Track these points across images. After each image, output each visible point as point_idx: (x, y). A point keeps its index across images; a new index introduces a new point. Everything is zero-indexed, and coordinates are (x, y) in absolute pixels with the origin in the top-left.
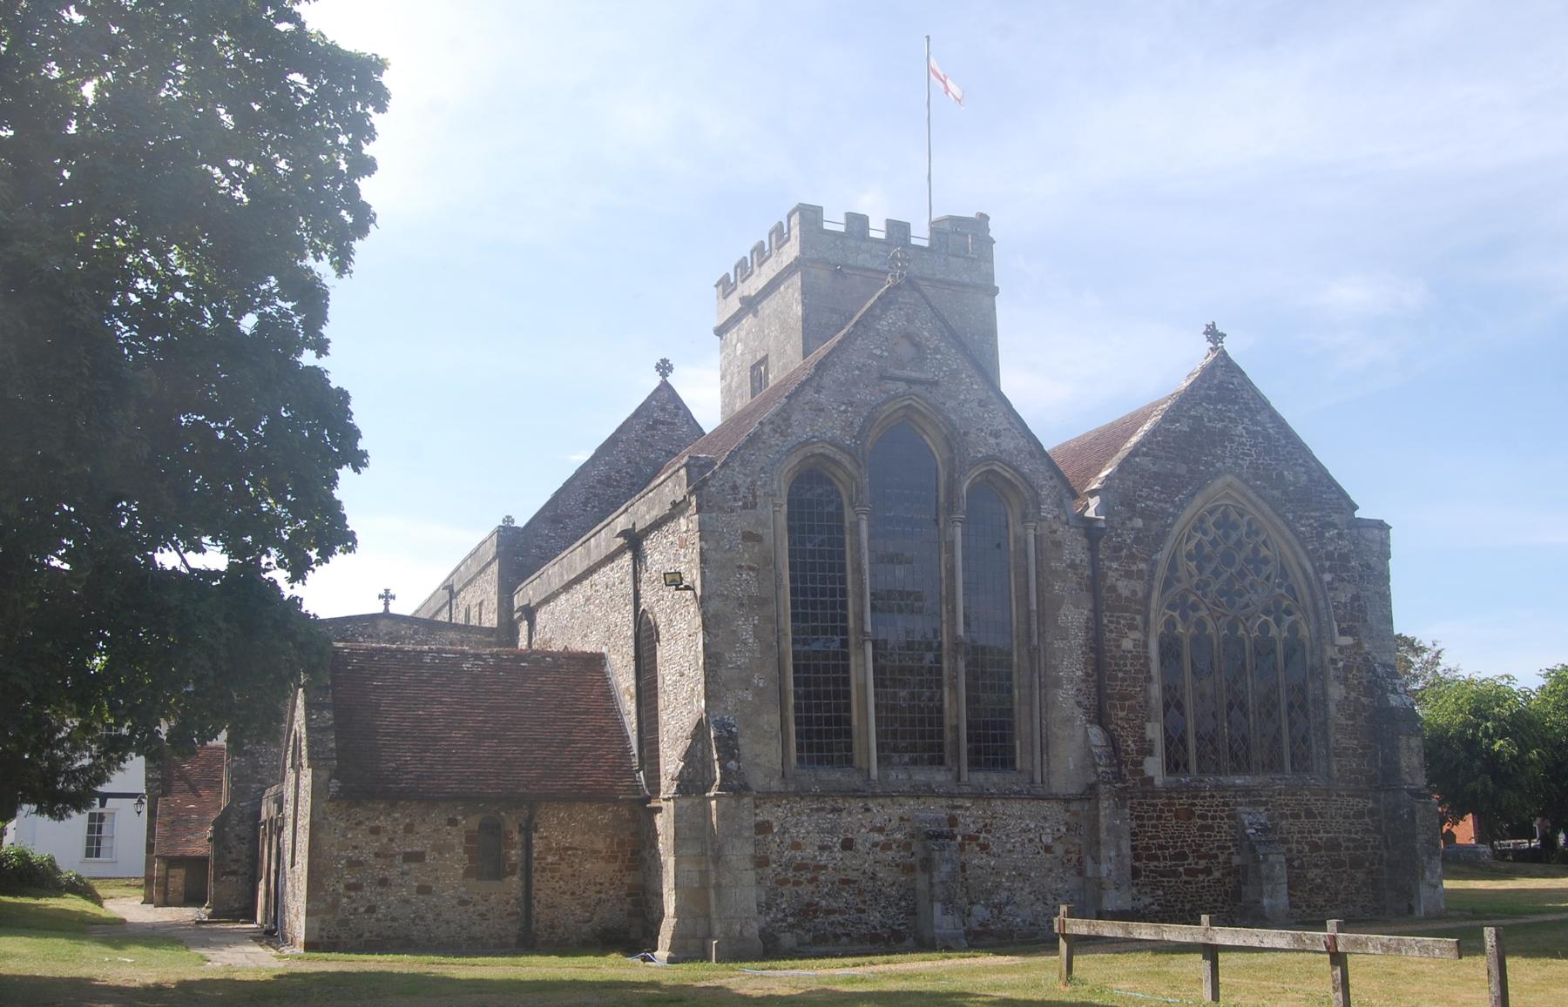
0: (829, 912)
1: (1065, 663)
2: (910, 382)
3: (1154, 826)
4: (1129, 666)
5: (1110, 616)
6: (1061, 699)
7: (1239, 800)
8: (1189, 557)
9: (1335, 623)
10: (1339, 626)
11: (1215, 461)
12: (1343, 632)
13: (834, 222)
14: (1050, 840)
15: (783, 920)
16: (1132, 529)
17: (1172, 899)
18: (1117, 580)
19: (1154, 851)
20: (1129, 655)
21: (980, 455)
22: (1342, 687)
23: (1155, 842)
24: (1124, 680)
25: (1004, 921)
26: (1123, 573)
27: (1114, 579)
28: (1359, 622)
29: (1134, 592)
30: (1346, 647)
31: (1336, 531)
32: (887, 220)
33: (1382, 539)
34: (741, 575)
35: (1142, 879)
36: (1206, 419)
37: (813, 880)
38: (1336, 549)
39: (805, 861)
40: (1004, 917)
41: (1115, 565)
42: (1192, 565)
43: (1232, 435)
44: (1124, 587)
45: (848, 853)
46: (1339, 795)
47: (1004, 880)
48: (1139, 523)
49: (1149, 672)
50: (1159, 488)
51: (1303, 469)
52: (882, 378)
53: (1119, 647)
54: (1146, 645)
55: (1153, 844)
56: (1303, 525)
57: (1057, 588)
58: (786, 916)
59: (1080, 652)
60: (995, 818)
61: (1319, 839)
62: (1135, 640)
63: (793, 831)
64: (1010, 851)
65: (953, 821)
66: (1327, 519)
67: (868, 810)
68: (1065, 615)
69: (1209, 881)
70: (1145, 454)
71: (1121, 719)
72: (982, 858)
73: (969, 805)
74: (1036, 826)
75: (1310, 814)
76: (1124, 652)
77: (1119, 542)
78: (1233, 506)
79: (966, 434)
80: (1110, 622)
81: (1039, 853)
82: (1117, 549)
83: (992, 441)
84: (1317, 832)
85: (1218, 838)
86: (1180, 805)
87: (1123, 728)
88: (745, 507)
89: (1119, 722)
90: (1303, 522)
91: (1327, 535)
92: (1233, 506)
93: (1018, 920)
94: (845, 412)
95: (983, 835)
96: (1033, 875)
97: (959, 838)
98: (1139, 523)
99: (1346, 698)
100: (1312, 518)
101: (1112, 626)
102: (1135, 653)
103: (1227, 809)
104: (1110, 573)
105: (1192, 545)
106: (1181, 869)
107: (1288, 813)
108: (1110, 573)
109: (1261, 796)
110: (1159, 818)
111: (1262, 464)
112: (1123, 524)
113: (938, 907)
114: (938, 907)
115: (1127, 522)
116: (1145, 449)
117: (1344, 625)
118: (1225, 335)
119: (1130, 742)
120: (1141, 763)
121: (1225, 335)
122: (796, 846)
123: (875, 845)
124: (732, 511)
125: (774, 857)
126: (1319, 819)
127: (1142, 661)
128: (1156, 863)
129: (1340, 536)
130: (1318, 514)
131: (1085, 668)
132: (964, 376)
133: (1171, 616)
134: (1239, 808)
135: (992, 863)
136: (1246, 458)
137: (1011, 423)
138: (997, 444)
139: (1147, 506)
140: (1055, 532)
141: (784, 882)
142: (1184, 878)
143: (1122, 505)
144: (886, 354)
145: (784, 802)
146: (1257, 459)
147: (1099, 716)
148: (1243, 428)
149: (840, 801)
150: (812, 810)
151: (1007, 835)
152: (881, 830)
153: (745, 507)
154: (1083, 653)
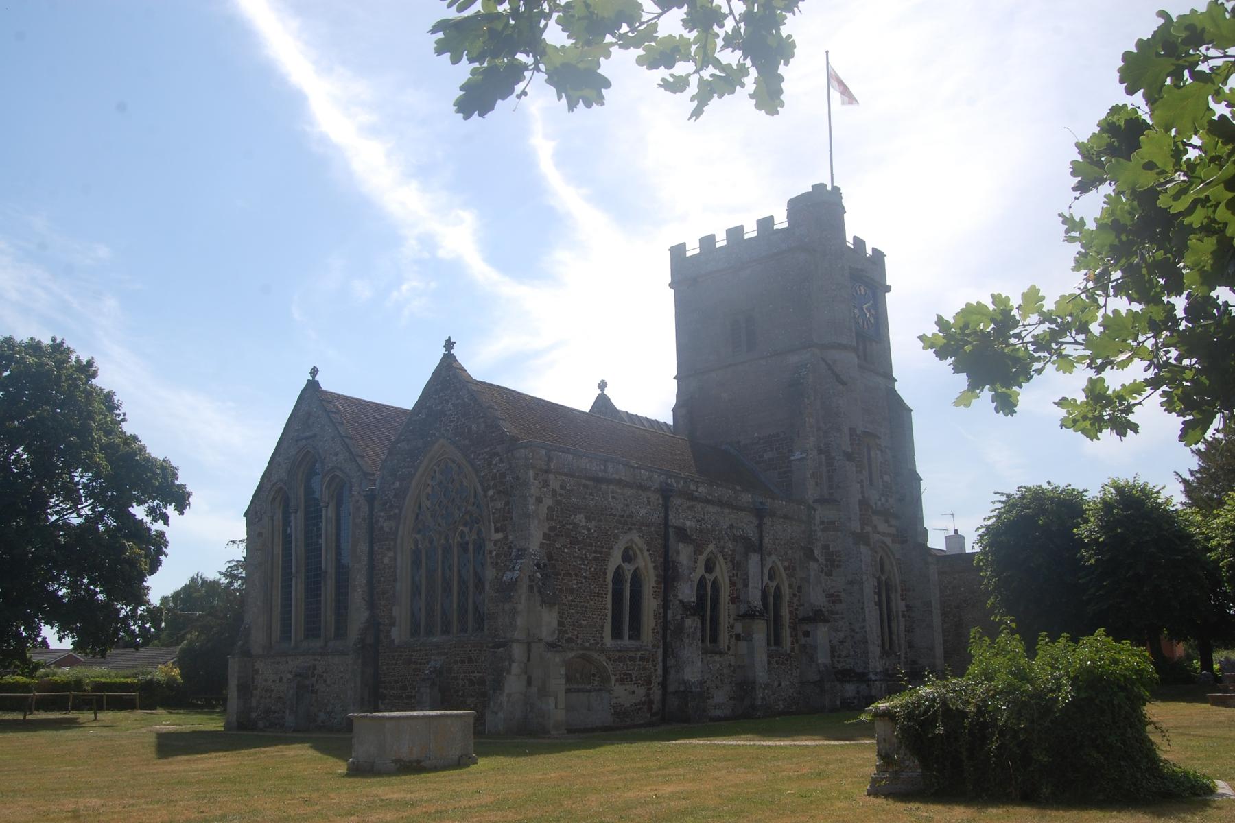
2: (307, 438)
3: (394, 669)
7: (433, 652)
9: (493, 525)
10: (495, 526)
12: (497, 530)
13: (693, 249)
18: (384, 522)
22: (494, 569)
28: (507, 520)
29: (391, 529)
30: (499, 541)
32: (714, 235)
33: (526, 455)
41: (382, 514)
46: (487, 647)
48: (397, 484)
51: (482, 420)
52: (297, 441)
53: (382, 562)
54: (395, 559)
56: (480, 460)
61: (475, 677)
65: (315, 668)
66: (494, 451)
67: (287, 662)
75: (470, 660)
78: (448, 458)
79: (325, 459)
80: (379, 548)
83: (334, 458)
84: (473, 672)
90: (480, 457)
91: (494, 462)
92: (448, 458)
98: (397, 484)
99: (496, 577)
100: (485, 453)
105: (429, 490)
108: (381, 519)
109: (445, 649)
113: (287, 711)
114: (287, 711)
116: (403, 437)
117: (499, 525)
121: (455, 343)
129: (501, 461)
137: (342, 445)
138: (337, 460)
140: (358, 501)
142: (406, 701)
146: (458, 422)
147: (372, 605)
153: (258, 521)
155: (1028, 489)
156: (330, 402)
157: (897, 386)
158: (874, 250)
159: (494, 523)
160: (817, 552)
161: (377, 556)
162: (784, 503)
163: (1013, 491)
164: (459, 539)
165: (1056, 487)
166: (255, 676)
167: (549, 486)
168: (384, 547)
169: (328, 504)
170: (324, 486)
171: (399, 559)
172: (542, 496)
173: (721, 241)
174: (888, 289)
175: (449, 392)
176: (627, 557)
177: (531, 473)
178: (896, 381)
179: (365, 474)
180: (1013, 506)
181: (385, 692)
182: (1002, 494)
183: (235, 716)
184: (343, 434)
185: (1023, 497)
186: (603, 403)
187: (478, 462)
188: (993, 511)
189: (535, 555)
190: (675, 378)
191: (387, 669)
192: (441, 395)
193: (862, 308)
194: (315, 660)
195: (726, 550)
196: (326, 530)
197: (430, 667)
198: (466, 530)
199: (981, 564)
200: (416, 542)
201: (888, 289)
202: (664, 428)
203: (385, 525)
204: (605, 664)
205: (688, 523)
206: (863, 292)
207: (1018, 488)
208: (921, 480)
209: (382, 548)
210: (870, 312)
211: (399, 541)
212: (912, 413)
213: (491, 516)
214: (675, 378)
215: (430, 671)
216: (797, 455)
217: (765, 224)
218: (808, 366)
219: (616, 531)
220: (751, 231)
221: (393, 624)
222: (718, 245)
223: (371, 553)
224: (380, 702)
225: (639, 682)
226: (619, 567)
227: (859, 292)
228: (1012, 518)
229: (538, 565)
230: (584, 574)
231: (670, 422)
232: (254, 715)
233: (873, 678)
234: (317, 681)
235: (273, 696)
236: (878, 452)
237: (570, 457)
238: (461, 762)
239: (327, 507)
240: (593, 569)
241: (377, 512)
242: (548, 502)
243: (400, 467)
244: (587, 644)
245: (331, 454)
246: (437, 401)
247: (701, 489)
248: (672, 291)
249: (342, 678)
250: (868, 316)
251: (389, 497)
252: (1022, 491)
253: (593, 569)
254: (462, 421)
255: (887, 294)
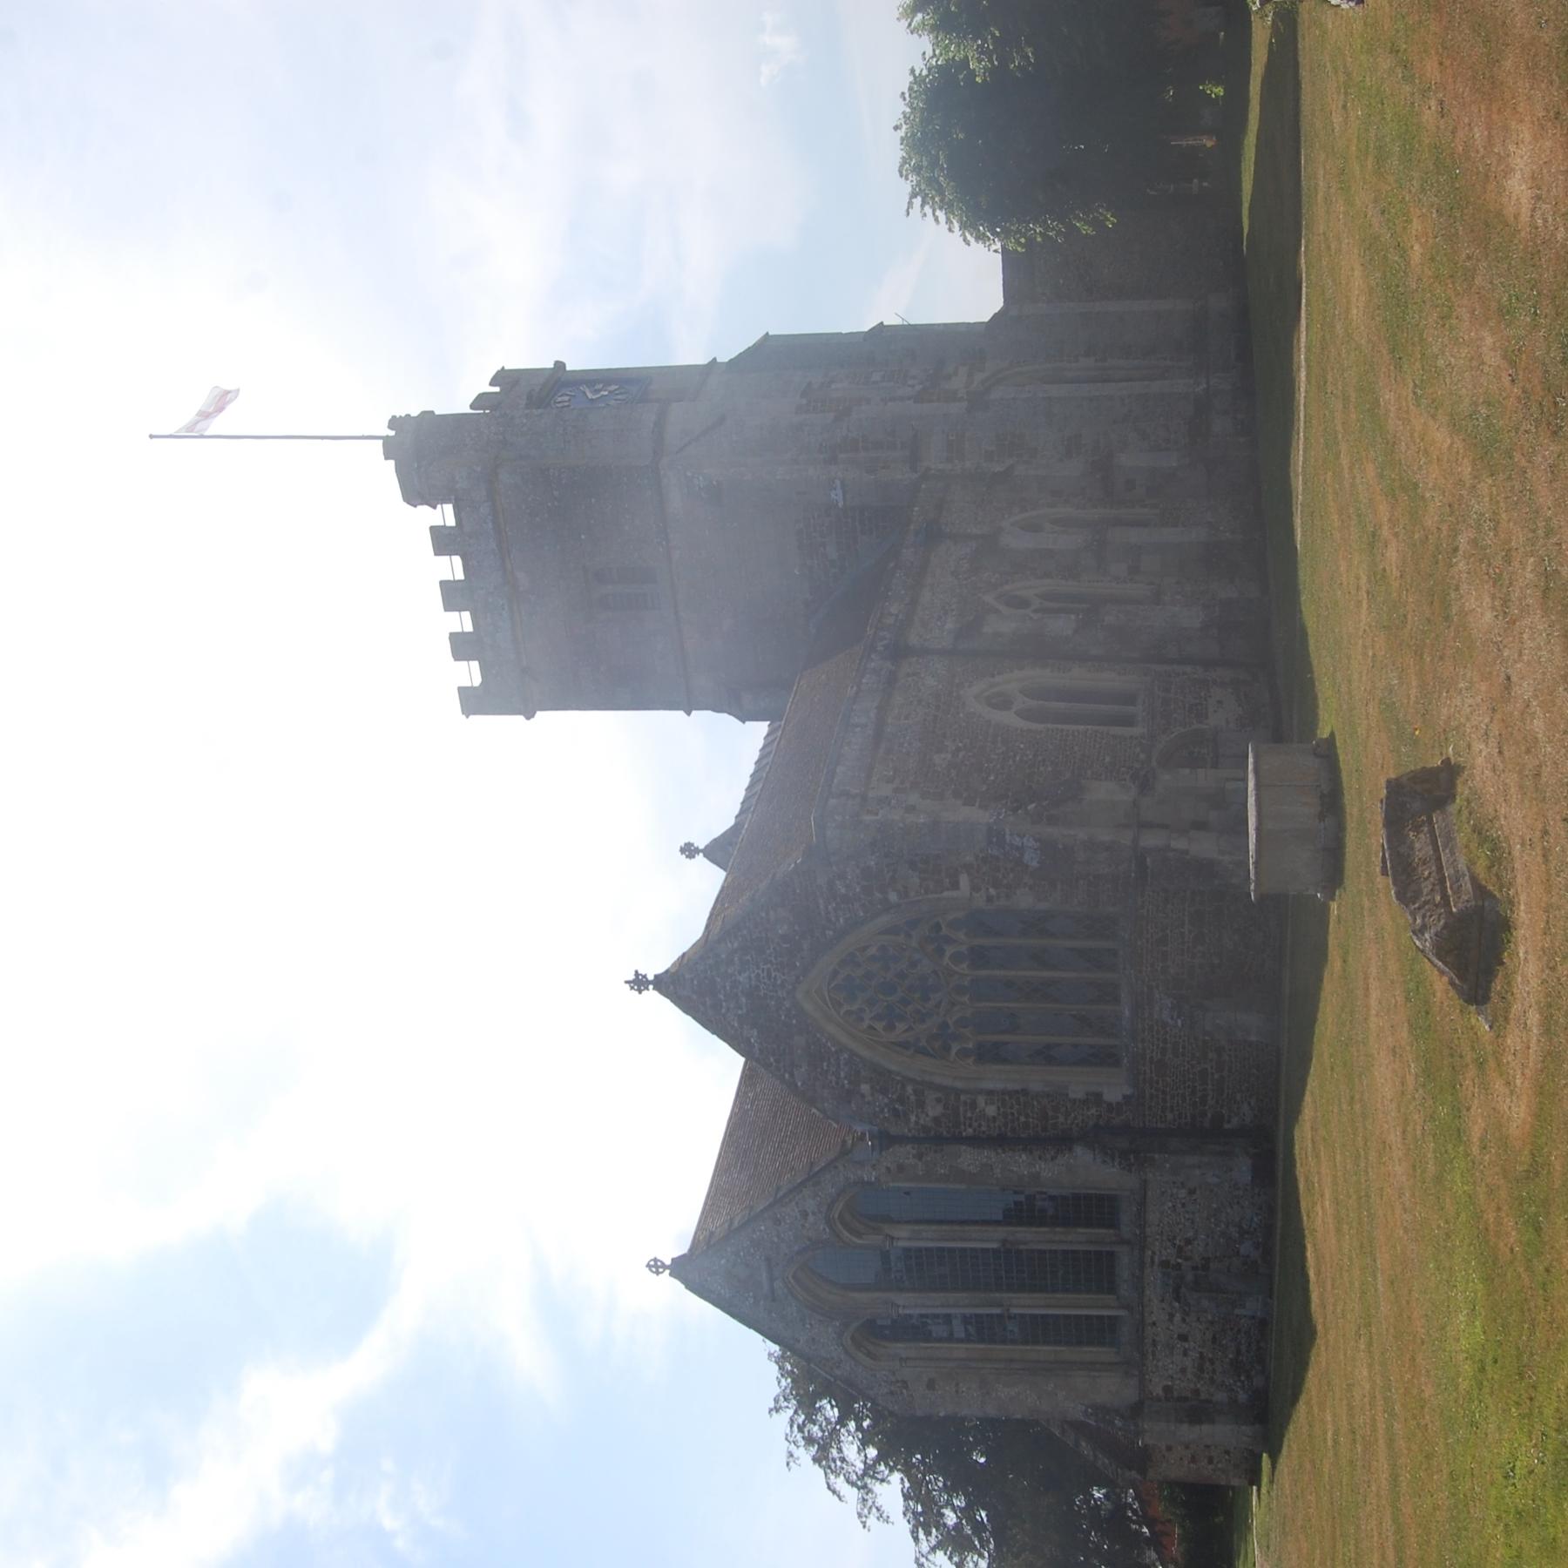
0: (1238, 1352)
1: (1015, 1169)
4: (1013, 1111)
5: (965, 1125)
6: (1050, 1175)
8: (890, 1027)
9: (946, 894)
10: (948, 889)
11: (783, 1008)
12: (955, 885)
14: (1183, 1191)
15: (1243, 1382)
16: (872, 1095)
17: (1246, 1085)
18: (927, 1115)
19: (1197, 1100)
20: (1002, 1110)
21: (827, 1230)
23: (1188, 1098)
24: (1027, 1116)
25: (1255, 1229)
26: (920, 1110)
27: (928, 1119)
29: (938, 1100)
31: (837, 882)
34: (963, 1392)
35: (1224, 1112)
36: (740, 1012)
37: (1212, 1362)
38: (858, 883)
39: (1196, 1365)
40: (1252, 1229)
41: (913, 1118)
42: (901, 1026)
43: (750, 986)
44: (934, 1110)
45: (1190, 1338)
47: (1219, 1229)
49: (1017, 1092)
50: (825, 1064)
51: (772, 913)
54: (990, 1093)
55: (1190, 1099)
57: (942, 1171)
58: (1240, 1380)
59: (1003, 1155)
60: (1162, 1232)
62: (986, 1103)
63: (1170, 1372)
64: (1193, 1223)
65: (1165, 1264)
67: (1154, 1324)
68: (969, 1165)
69: (1230, 1050)
70: (792, 1075)
71: (1066, 1119)
72: (1198, 1244)
73: (1150, 1252)
74: (1171, 1201)
76: (999, 1114)
77: (889, 1111)
78: (829, 984)
79: (809, 1239)
80: (970, 1126)
81: (1195, 1200)
82: (896, 1113)
83: (811, 1218)
85: (1186, 1039)
86: (1151, 1073)
87: (1075, 1118)
88: (907, 1388)
89: (1069, 1122)
91: (843, 891)
92: (829, 984)
93: (1255, 1219)
94: (811, 1324)
95: (1177, 1242)
96: (1215, 1206)
97: (1179, 1261)
98: (865, 1088)
101: (975, 1124)
102: (1000, 1104)
103: (1156, 1028)
104: (922, 1122)
105: (879, 1026)
106: (1216, 1076)
107: (1161, 965)
108: (922, 1122)
110: (1164, 1092)
111: (776, 958)
112: (869, 1103)
115: (866, 1100)
116: (787, 1076)
118: (636, 972)
119: (1089, 1113)
120: (1110, 1104)
121: (636, 972)
122: (1183, 1371)
123: (1184, 1320)
124: (912, 1395)
125: (1192, 1386)
126: (1168, 932)
127: (1007, 1098)
128: (1209, 1098)
130: (821, 901)
131: (1019, 1150)
132: (755, 1236)
133: (956, 1054)
134: (1156, 1017)
135: (1203, 1237)
136: (773, 975)
137: (791, 1201)
138: (814, 1213)
139: (846, 1078)
140: (888, 1169)
141: (1212, 1381)
143: (850, 1102)
144: (751, 1294)
145: (1147, 1377)
146: (771, 962)
147: (1063, 1141)
148: (740, 975)
149: (1146, 1341)
150: (1153, 1359)
151: (1178, 1224)
152: (1171, 1316)
153: (907, 1388)
154: (1004, 1153)
155: (904, 161)
156: (712, 1233)
157: (724, 358)
158: (492, 384)
159: (942, 892)
160: (998, 468)
161: (983, 1129)
162: (916, 509)
163: (906, 187)
164: (964, 966)
165: (905, 117)
166: (1176, 1394)
167: (887, 797)
168: (969, 1115)
169: (887, 1235)
170: (859, 1241)
171: (990, 1085)
172: (904, 805)
173: (463, 622)
174: (560, 365)
175: (719, 980)
176: (1004, 703)
177: (867, 818)
178: (715, 359)
179: (845, 1152)
180: (932, 182)
181: (1209, 1115)
182: (910, 204)
183: (1244, 1428)
184: (771, 1200)
185: (917, 169)
186: (717, 852)
187: (841, 920)
188: (936, 219)
189: (999, 814)
190: (689, 714)
191: (1172, 1110)
192: (722, 997)
193: (592, 399)
194: (1153, 1262)
195: (993, 580)
196: (932, 1240)
197: (1172, 1018)
198: (949, 950)
199: (1023, 240)
200: (964, 1053)
201: (560, 365)
202: (770, 739)
203: (931, 1114)
204: (1173, 735)
205: (949, 626)
206: (566, 398)
207: (901, 176)
208: (882, 323)
209: (971, 1119)
210: (600, 390)
211: (959, 1085)
212: (770, 333)
213: (930, 896)
214: (689, 714)
215: (1179, 1017)
216: (837, 496)
217: (443, 541)
218: (689, 474)
219: (961, 715)
220: (452, 567)
221: (1098, 1097)
222: (469, 627)
223: (976, 1141)
224: (1226, 1126)
225: (1202, 694)
226: (1018, 714)
227: (566, 404)
228: (952, 184)
229: (1015, 810)
230: (1031, 757)
231: (760, 729)
232: (1242, 1397)
233: (1205, 386)
234: (1187, 1259)
235: (1210, 1356)
236: (833, 386)
237: (840, 769)
238: (1327, 754)
239: (892, 1238)
240: (1022, 746)
241: (910, 1131)
242: (913, 798)
243: (837, 1083)
244: (1142, 756)
245: (803, 1226)
246: (732, 1006)
247: (894, 610)
248: (539, 714)
249: (1183, 1205)
250: (606, 393)
251: (886, 1105)
252: (906, 170)
253: (1022, 746)
254: (770, 956)
255: (568, 368)
